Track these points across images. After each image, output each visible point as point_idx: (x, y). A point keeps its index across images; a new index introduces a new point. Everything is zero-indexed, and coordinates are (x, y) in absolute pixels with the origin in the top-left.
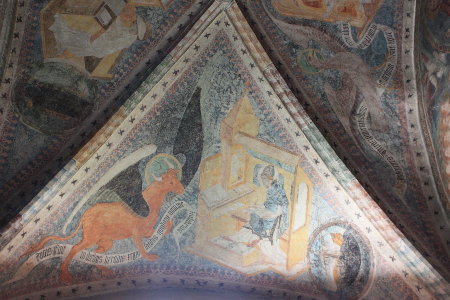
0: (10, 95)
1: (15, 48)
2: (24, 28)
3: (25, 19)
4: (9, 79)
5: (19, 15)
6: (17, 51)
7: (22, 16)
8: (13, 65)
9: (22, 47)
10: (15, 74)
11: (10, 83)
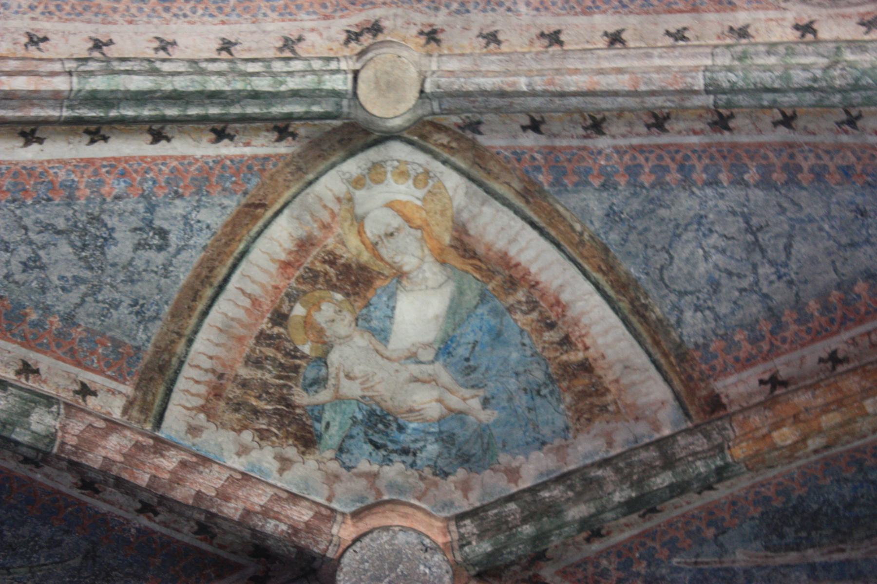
0: (862, 10)
1: (668, 33)
2: (582, 20)
3: (549, 22)
4: (797, 27)
5: (531, 43)
6: (680, 26)
7: (535, 31)
8: (737, 26)
9: (658, 13)
10: (772, 14)
11: (812, 22)
